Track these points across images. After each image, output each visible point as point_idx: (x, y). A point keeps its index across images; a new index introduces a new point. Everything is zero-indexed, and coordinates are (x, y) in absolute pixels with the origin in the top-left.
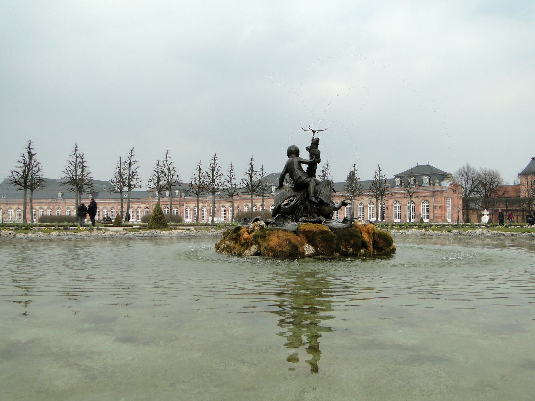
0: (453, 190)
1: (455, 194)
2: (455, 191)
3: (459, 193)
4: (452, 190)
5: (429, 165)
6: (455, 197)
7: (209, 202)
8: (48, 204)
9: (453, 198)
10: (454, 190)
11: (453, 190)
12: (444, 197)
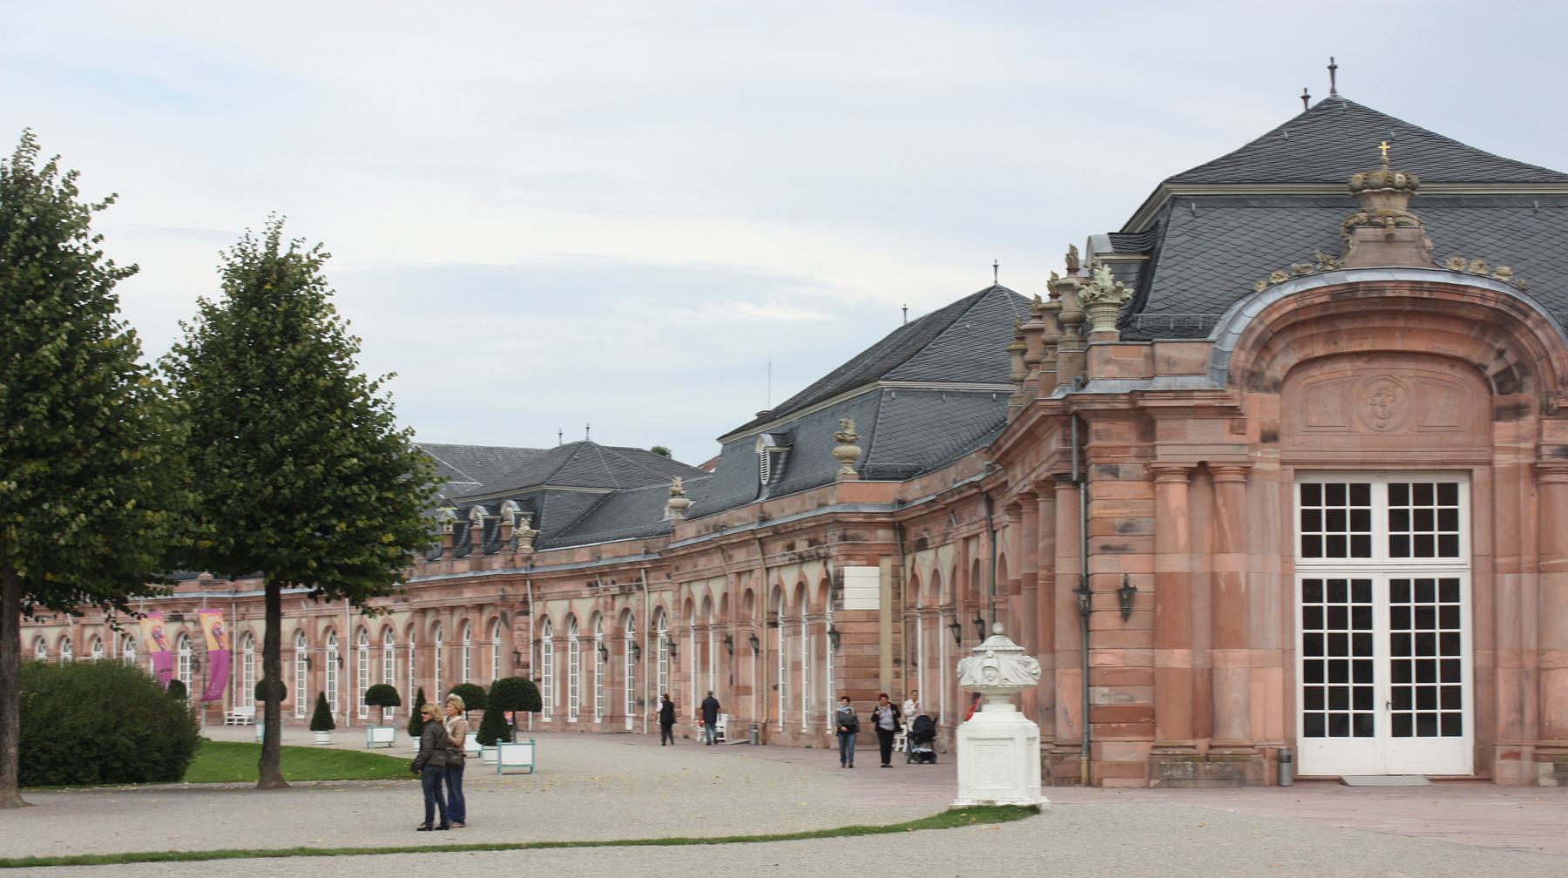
2: (1507, 381)
3: (1547, 411)
4: (1458, 374)
5: (1344, 93)
6: (1503, 460)
7: (608, 579)
9: (1480, 473)
10: (1493, 368)
11: (1478, 369)
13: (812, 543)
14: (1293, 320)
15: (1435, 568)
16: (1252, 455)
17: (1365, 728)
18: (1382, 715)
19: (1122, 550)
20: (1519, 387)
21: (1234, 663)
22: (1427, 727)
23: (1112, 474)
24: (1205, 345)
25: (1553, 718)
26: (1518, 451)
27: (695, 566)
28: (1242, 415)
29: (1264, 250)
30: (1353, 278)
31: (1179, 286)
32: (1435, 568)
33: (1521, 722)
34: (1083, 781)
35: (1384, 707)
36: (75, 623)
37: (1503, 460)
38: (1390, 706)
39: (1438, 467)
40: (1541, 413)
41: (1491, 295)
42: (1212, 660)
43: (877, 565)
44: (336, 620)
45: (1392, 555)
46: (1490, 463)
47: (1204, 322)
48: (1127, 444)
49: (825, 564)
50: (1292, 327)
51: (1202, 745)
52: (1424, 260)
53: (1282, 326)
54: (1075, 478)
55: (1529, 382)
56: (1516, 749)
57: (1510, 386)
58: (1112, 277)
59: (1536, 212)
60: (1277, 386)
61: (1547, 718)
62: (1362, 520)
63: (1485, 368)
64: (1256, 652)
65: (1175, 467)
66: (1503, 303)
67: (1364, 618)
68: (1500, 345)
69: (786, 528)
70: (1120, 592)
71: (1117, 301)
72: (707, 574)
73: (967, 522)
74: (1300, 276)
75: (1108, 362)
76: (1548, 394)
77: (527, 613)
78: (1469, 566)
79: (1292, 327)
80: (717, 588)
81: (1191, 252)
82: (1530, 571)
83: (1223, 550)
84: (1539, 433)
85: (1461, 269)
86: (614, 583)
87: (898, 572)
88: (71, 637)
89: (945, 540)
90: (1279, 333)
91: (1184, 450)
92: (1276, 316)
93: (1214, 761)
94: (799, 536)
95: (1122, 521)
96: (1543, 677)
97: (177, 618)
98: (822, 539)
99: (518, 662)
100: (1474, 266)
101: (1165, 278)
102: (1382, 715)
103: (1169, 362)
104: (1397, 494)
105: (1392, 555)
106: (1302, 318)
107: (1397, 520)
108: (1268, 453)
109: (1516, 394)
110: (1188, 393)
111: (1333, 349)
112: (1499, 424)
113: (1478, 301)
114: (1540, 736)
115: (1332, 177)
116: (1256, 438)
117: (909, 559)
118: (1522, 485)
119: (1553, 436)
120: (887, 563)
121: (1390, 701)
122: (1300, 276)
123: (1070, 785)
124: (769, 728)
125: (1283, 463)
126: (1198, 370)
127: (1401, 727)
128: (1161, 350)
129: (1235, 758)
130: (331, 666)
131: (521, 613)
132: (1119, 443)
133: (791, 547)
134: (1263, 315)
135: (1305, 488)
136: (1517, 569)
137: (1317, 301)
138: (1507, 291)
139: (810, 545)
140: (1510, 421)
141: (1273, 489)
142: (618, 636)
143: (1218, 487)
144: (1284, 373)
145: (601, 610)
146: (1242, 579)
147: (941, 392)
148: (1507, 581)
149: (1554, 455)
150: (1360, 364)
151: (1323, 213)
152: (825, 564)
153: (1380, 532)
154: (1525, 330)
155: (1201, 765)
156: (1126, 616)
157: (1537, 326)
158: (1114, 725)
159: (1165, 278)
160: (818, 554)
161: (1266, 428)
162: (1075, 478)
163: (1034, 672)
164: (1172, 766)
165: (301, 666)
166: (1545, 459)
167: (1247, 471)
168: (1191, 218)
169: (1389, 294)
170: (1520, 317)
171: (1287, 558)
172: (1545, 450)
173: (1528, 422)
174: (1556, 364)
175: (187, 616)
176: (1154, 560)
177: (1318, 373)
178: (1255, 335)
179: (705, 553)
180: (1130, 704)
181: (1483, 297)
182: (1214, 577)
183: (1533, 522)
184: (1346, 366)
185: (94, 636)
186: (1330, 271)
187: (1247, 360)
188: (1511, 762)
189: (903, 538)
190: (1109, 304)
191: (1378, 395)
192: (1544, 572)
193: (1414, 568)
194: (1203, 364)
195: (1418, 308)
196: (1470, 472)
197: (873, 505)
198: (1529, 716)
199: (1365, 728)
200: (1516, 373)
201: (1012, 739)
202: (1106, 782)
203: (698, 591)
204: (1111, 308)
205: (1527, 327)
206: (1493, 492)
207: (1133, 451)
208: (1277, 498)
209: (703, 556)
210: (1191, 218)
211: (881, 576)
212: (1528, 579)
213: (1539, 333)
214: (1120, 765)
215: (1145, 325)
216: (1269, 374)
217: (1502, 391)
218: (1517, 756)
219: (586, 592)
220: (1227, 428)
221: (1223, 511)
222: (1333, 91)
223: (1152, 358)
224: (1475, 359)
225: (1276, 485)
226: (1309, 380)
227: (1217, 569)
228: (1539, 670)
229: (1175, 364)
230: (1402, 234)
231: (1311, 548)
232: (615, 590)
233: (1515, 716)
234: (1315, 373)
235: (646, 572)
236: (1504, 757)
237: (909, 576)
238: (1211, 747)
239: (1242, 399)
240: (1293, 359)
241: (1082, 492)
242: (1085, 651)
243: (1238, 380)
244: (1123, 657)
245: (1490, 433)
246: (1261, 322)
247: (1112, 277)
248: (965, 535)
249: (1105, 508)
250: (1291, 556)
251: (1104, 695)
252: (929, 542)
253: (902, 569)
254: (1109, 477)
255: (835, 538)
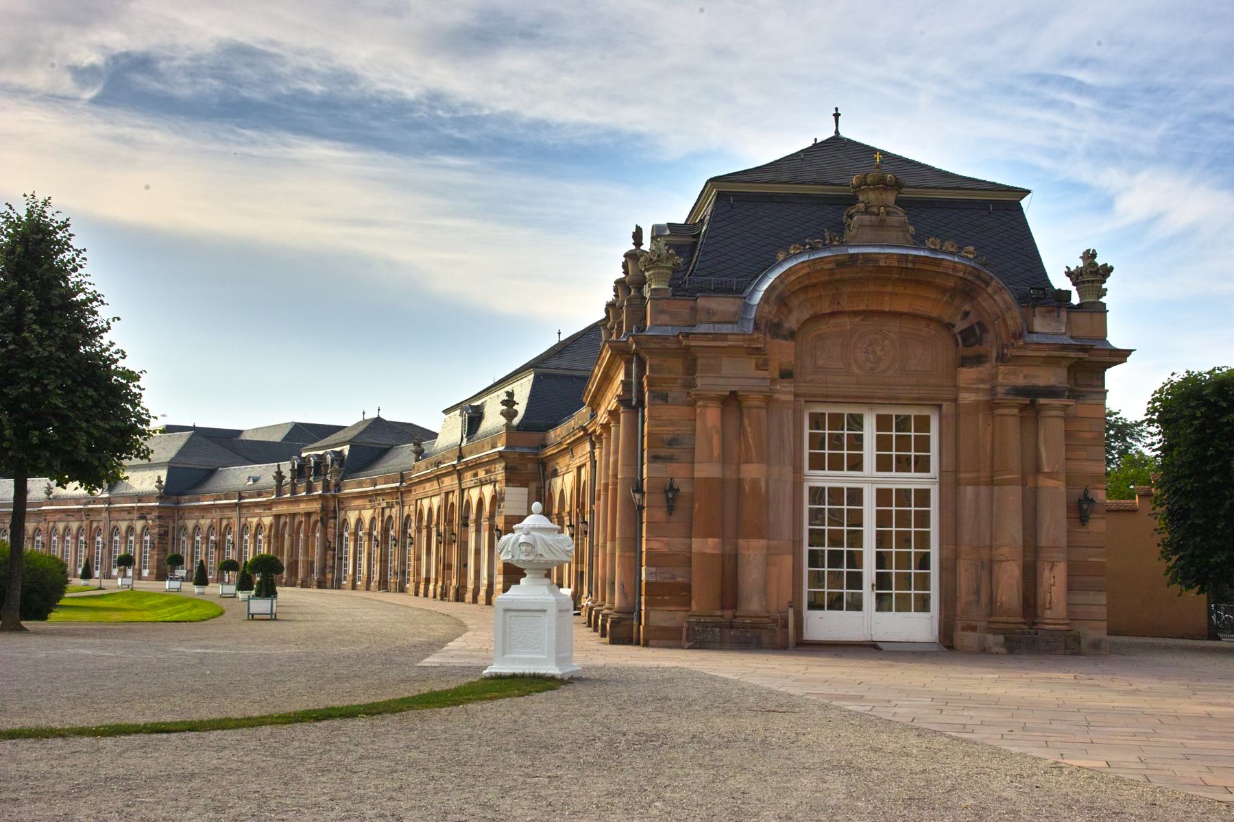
0: (949, 326)
1: (968, 375)
2: (971, 336)
3: (1002, 359)
5: (844, 133)
6: (966, 398)
8: (78, 515)
10: (960, 326)
11: (949, 326)
12: (731, 401)
13: (487, 472)
14: (807, 282)
15: (911, 480)
16: (774, 387)
17: (856, 605)
18: (869, 595)
19: (669, 459)
20: (980, 341)
21: (752, 551)
22: (903, 605)
23: (662, 399)
24: (738, 301)
25: (1004, 600)
26: (978, 390)
27: (424, 489)
28: (765, 355)
29: (784, 234)
30: (851, 251)
31: (720, 259)
32: (911, 480)
33: (978, 602)
34: (634, 641)
35: (870, 588)
36: (87, 519)
37: (966, 398)
38: (875, 587)
39: (916, 402)
40: (997, 361)
41: (960, 266)
42: (736, 547)
43: (526, 486)
44: (232, 521)
45: (879, 469)
46: (956, 400)
47: (737, 285)
48: (675, 376)
49: (495, 486)
50: (805, 289)
51: (728, 613)
52: (907, 240)
53: (798, 287)
54: (634, 403)
55: (990, 336)
56: (973, 623)
57: (972, 340)
58: (667, 247)
59: (990, 213)
60: (792, 335)
61: (999, 600)
62: (857, 442)
63: (954, 326)
64: (774, 542)
65: (712, 394)
66: (970, 273)
67: (856, 519)
68: (967, 307)
69: (472, 462)
70: (666, 492)
71: (670, 265)
72: (430, 493)
73: (580, 455)
74: (812, 248)
75: (662, 312)
76: (1004, 346)
77: (335, 518)
78: (938, 480)
79: (805, 289)
80: (436, 501)
81: (730, 234)
82: (986, 484)
83: (748, 461)
84: (995, 376)
85: (938, 247)
86: (383, 500)
87: (541, 491)
88: (84, 527)
89: (568, 469)
90: (794, 293)
91: (720, 381)
92: (793, 278)
93: (737, 628)
94: (480, 468)
95: (670, 437)
96: (996, 567)
97: (143, 517)
98: (493, 470)
99: (329, 547)
100: (948, 245)
101: (709, 252)
102: (869, 595)
103: (709, 312)
104: (883, 422)
105: (879, 469)
106: (813, 281)
107: (883, 443)
108: (786, 387)
109: (977, 346)
110: (723, 337)
111: (836, 308)
112: (964, 370)
113: (951, 272)
114: (991, 614)
115: (836, 182)
116: (776, 374)
117: (547, 482)
118: (980, 416)
119: (1006, 378)
120: (533, 486)
121: (875, 583)
122: (814, 249)
123: (623, 643)
124: (460, 591)
125: (796, 395)
126: (732, 319)
127: (882, 603)
128: (702, 302)
129: (753, 626)
130: (229, 548)
131: (331, 518)
132: (669, 376)
133: (476, 475)
134: (783, 276)
135: (812, 416)
136: (976, 483)
137: (826, 267)
138: (972, 264)
139: (486, 474)
140: (972, 367)
141: (788, 415)
142: (385, 531)
143: (745, 411)
144: (798, 326)
145: (376, 516)
146: (763, 484)
147: (572, 377)
148: (969, 491)
149: (1007, 393)
150: (857, 320)
151: (831, 208)
152: (495, 486)
153: (869, 452)
154: (986, 295)
155: (726, 631)
156: (671, 509)
157: (995, 292)
158: (659, 598)
159: (709, 252)
160: (490, 479)
161: (784, 368)
162: (634, 403)
163: (568, 549)
164: (703, 631)
165: (212, 548)
166: (999, 396)
167: (769, 400)
168: (730, 209)
169: (882, 264)
170: (983, 286)
171: (798, 470)
172: (1000, 390)
173: (984, 370)
174: (1010, 322)
175: (148, 517)
176: (693, 467)
177: (825, 327)
178: (776, 293)
179: (429, 480)
180: (672, 581)
181: (955, 269)
182: (740, 482)
183: (989, 447)
184: (846, 321)
185: (97, 527)
186: (836, 246)
187: (770, 312)
188: (971, 634)
189: (544, 470)
190: (664, 267)
191: (870, 345)
192: (997, 485)
193: (897, 480)
194: (735, 315)
195: (903, 277)
196: (940, 407)
197: (526, 447)
198: (984, 598)
199: (856, 605)
200: (977, 329)
201: (544, 611)
202: (651, 642)
203: (426, 503)
204: (665, 271)
205: (988, 293)
206: (957, 424)
207: (679, 382)
208: (791, 424)
209: (428, 482)
210: (730, 209)
211: (529, 493)
212: (984, 490)
213: (997, 297)
214: (663, 629)
215: (691, 286)
216: (786, 325)
217: (965, 345)
218: (974, 629)
219: (368, 504)
220: (753, 365)
221: (749, 430)
222: (837, 132)
223: (694, 309)
224: (946, 319)
225: (791, 412)
226: (818, 332)
227: (742, 476)
228: (991, 561)
229: (714, 314)
230: (894, 220)
231: (817, 463)
232: (384, 504)
233: (973, 598)
234: (823, 328)
235: (401, 494)
236: (963, 629)
237: (547, 494)
238: (735, 617)
239: (766, 343)
240: (806, 315)
241: (640, 414)
242: (638, 538)
243: (763, 327)
244: (667, 544)
245: (955, 377)
246: (782, 282)
247: (667, 247)
248: (578, 465)
249: (656, 426)
250: (801, 468)
251: (652, 574)
252: (559, 471)
253: (543, 490)
254: (661, 402)
255: (500, 468)
